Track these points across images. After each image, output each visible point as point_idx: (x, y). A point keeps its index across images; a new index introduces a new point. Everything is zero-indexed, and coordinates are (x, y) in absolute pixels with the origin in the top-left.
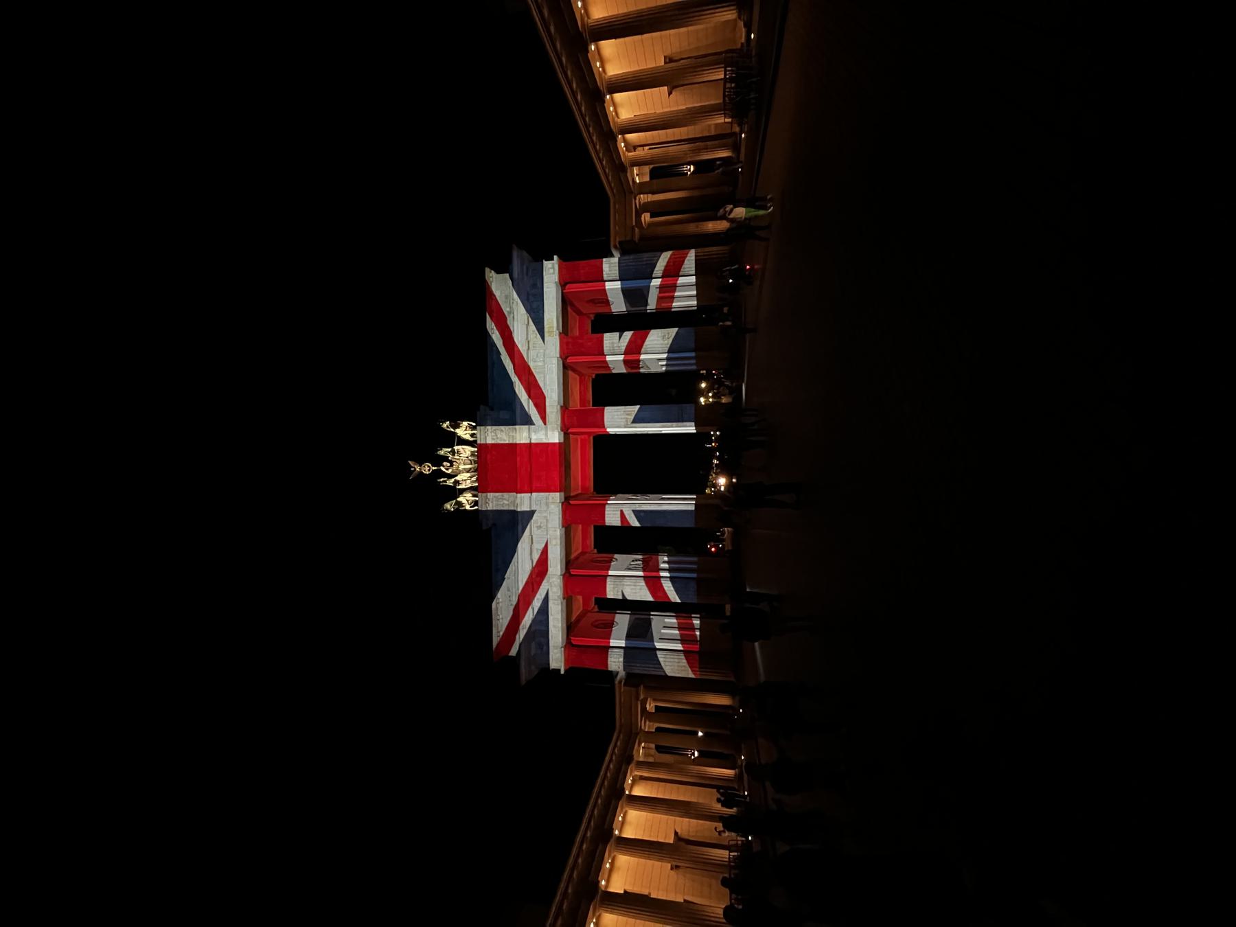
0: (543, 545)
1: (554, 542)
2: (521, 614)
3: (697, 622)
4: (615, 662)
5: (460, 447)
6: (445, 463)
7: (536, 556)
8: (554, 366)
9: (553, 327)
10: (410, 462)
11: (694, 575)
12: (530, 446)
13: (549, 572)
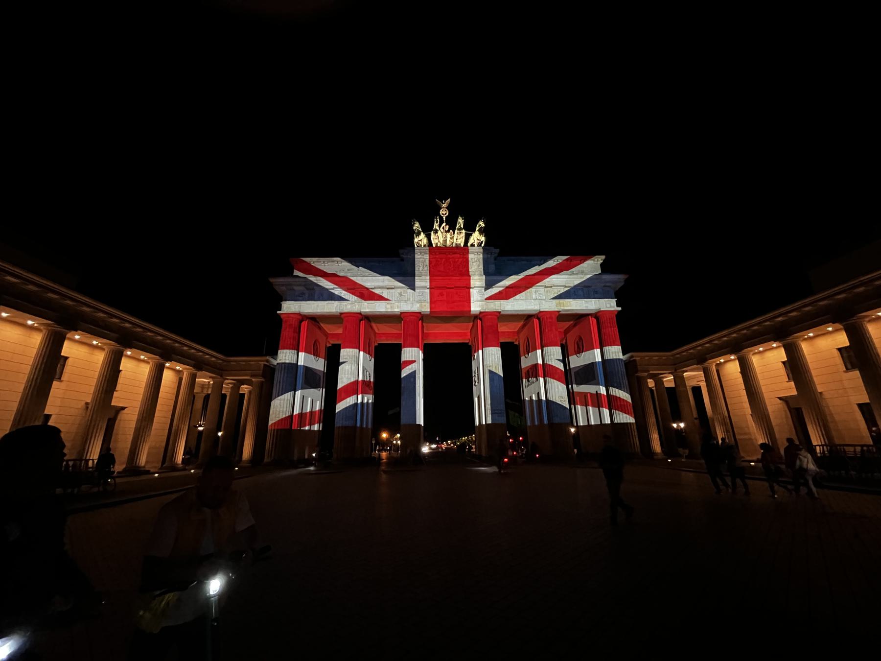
0: (386, 297)
1: (389, 306)
2: (327, 278)
3: (316, 427)
4: (285, 357)
5: (464, 234)
6: (448, 227)
7: (377, 291)
8: (533, 307)
10: (449, 200)
11: (358, 425)
12: (468, 287)
13: (363, 301)
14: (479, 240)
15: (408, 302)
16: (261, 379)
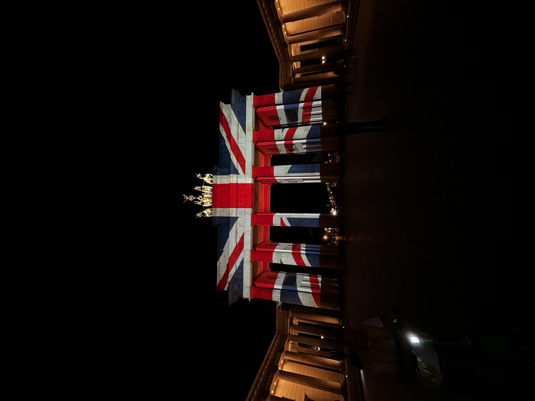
1: (247, 233)
3: (320, 279)
4: (277, 297)
6: (200, 196)
7: (238, 240)
9: (250, 127)
10: (184, 195)
11: (319, 253)
12: (237, 184)
13: (244, 248)
14: (208, 178)
16: (290, 312)
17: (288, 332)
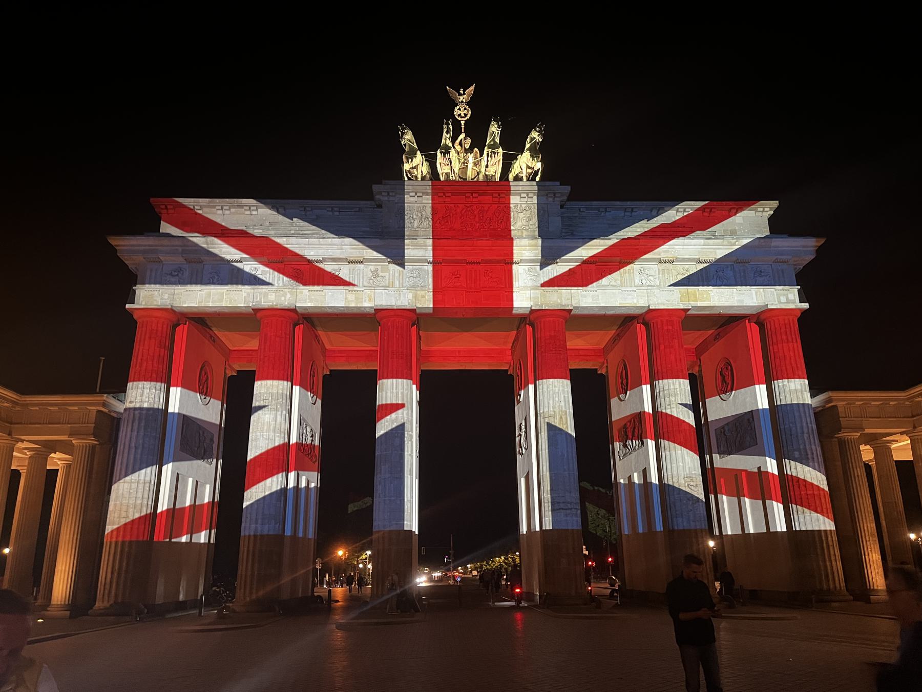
1: (351, 297)
3: (202, 537)
4: (142, 395)
5: (500, 157)
6: (469, 141)
7: (328, 267)
10: (472, 88)
11: (288, 532)
12: (508, 262)
13: (301, 287)
14: (530, 168)
15: (390, 289)
16: (91, 441)
17: (23, 437)
